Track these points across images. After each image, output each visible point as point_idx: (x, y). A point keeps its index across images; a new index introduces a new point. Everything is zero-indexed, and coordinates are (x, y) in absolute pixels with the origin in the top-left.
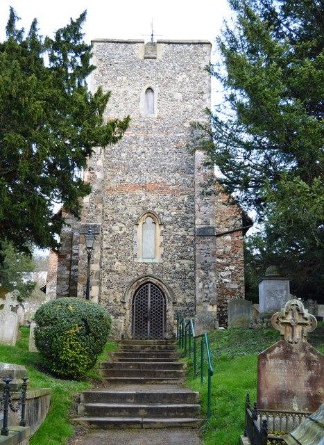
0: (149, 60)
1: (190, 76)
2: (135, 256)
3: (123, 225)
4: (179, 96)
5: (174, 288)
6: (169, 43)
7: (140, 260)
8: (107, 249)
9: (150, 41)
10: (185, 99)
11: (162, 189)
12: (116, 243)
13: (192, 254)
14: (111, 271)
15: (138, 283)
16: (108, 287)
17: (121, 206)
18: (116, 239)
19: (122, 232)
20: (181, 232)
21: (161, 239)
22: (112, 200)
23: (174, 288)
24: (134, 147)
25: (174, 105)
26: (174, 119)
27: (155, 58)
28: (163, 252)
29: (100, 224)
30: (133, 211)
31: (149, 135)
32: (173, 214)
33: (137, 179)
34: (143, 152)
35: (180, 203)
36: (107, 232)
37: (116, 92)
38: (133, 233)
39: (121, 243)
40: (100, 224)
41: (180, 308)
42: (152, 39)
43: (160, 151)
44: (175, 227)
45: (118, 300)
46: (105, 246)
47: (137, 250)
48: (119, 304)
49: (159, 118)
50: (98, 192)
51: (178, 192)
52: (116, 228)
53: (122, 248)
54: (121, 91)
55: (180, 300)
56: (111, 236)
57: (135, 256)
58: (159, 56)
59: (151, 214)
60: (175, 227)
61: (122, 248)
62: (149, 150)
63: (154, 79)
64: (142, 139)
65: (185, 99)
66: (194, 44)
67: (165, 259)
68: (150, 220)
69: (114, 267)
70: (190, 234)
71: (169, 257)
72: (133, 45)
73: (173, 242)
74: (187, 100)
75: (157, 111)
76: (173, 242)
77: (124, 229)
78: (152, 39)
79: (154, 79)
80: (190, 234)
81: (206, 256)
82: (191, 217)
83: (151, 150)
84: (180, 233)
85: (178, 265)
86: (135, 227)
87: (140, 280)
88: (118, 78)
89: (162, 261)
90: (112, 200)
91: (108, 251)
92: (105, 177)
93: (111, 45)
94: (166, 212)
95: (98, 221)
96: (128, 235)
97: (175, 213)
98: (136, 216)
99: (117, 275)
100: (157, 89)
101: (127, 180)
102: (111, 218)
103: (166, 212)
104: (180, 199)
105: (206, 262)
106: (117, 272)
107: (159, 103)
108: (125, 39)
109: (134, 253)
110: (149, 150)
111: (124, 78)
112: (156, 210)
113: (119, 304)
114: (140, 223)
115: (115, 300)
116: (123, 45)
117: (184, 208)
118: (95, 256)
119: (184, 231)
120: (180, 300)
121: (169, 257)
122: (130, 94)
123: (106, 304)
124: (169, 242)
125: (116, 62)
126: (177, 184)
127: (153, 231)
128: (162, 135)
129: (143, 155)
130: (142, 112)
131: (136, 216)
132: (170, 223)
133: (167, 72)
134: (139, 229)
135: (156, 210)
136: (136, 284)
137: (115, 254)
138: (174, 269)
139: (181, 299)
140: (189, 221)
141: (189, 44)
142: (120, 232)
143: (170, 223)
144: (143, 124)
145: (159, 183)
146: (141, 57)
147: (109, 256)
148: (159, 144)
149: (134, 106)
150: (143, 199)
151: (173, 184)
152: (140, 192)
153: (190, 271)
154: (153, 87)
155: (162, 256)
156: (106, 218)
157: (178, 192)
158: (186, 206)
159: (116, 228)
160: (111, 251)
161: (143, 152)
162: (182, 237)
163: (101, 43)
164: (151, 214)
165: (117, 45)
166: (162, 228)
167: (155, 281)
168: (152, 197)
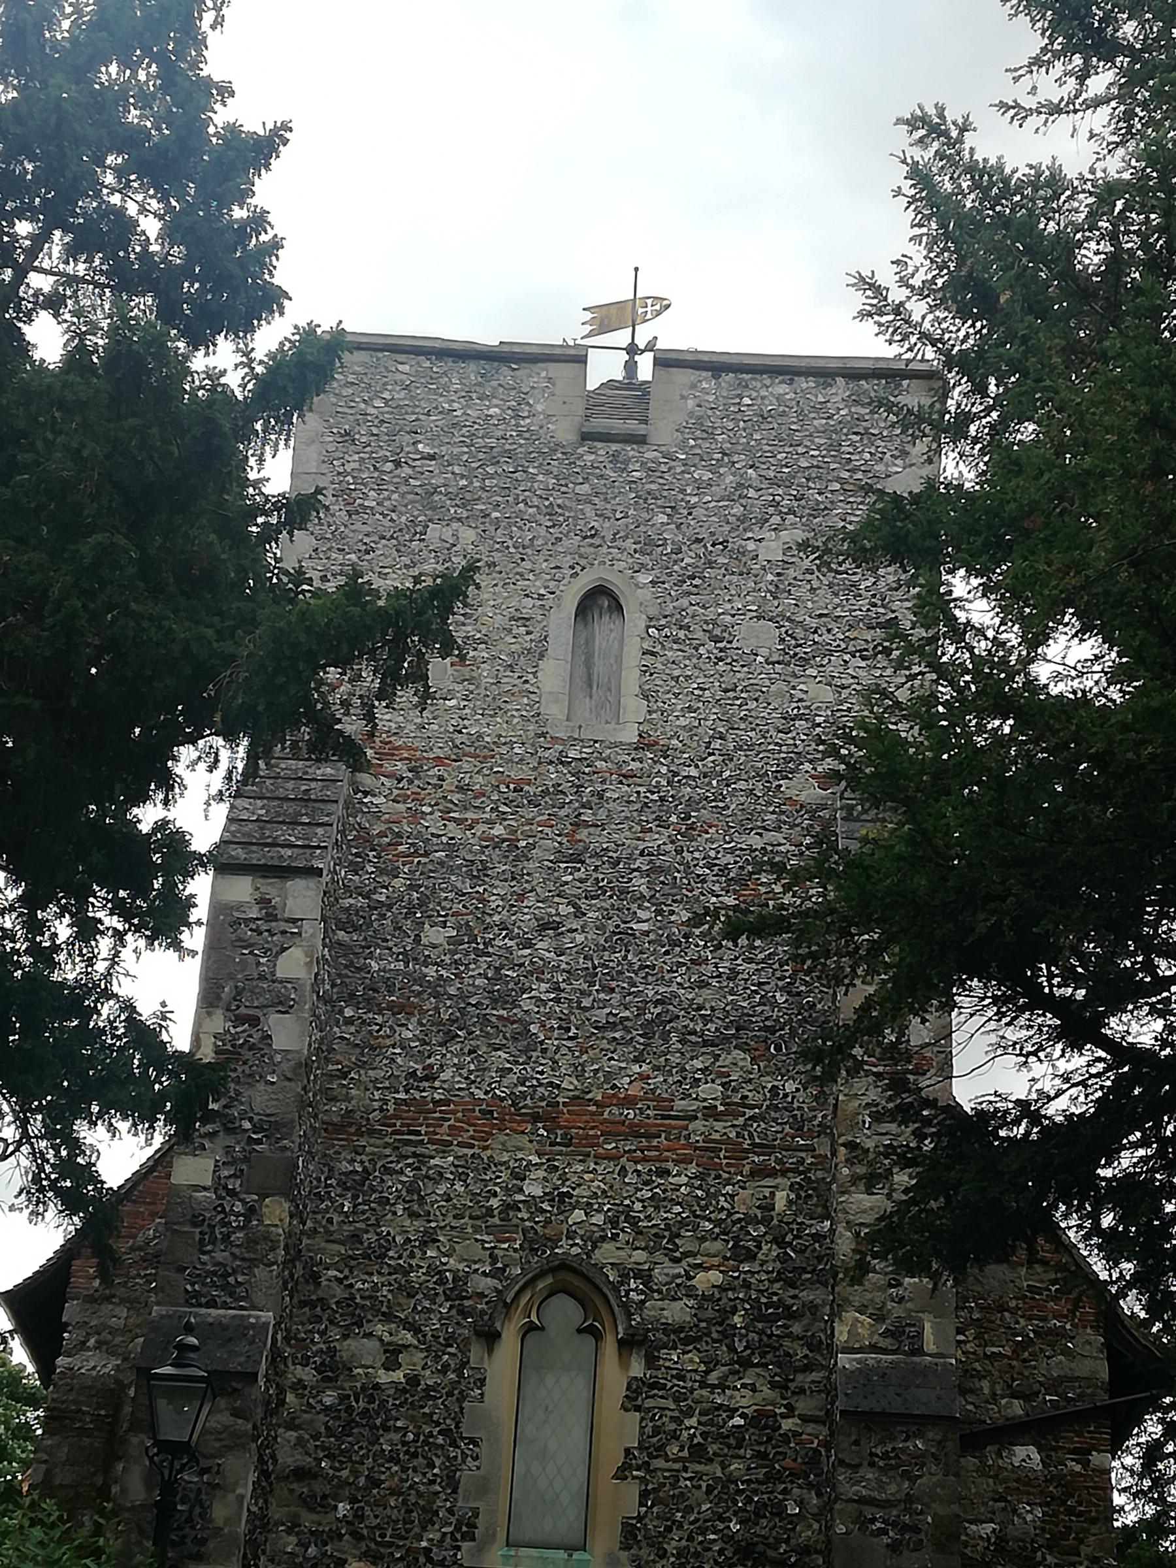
0: (602, 448)
3: (408, 1337)
4: (760, 638)
8: (301, 1474)
9: (619, 375)
10: (795, 657)
11: (647, 1133)
13: (807, 1534)
17: (400, 1225)
18: (362, 1414)
19: (399, 1376)
20: (746, 1397)
21: (623, 1430)
22: (356, 1184)
25: (729, 681)
27: (641, 440)
29: (268, 1316)
30: (467, 1256)
31: (583, 834)
32: (706, 1280)
34: (546, 926)
35: (749, 1219)
38: (466, 1385)
40: (268, 1316)
43: (644, 920)
44: (711, 1363)
46: (288, 1457)
47: (484, 1488)
49: (644, 744)
50: (271, 1128)
51: (738, 1154)
52: (364, 1351)
53: (391, 1475)
58: (664, 429)
59: (574, 1279)
60: (711, 1363)
61: (391, 1475)
62: (579, 913)
63: (629, 544)
64: (545, 851)
65: (795, 657)
67: (646, 1553)
68: (564, 1313)
70: (803, 1405)
71: (672, 1547)
73: (698, 1453)
74: (805, 662)
75: (634, 709)
76: (698, 1453)
79: (629, 544)
80: (803, 1405)
81: (894, 1547)
82: (813, 1308)
86: (476, 1353)
88: (434, 532)
91: (302, 1488)
92: (323, 1050)
94: (664, 1271)
95: (258, 1297)
97: (715, 1277)
98: (486, 1284)
100: (639, 596)
102: (339, 1292)
103: (664, 1271)
104: (746, 1199)
107: (645, 670)
108: (488, 337)
110: (579, 913)
111: (468, 535)
112: (606, 1254)
116: (471, 370)
117: (770, 1251)
118: (220, 1512)
119: (767, 1392)
121: (672, 1547)
124: (673, 1449)
126: (732, 1110)
127: (580, 1384)
128: (657, 840)
130: (554, 711)
131: (486, 1284)
132: (682, 1336)
133: (699, 512)
134: (502, 1365)
135: (606, 1254)
137: (343, 1508)
140: (796, 1328)
142: (383, 1377)
144: (553, 775)
145: (630, 1102)
146: (564, 432)
147: (308, 1520)
149: (510, 680)
151: (710, 1113)
154: (617, 582)
157: (738, 1154)
158: (779, 1241)
160: (319, 1487)
161: (546, 926)
166: (637, 1369)
168: (589, 1178)
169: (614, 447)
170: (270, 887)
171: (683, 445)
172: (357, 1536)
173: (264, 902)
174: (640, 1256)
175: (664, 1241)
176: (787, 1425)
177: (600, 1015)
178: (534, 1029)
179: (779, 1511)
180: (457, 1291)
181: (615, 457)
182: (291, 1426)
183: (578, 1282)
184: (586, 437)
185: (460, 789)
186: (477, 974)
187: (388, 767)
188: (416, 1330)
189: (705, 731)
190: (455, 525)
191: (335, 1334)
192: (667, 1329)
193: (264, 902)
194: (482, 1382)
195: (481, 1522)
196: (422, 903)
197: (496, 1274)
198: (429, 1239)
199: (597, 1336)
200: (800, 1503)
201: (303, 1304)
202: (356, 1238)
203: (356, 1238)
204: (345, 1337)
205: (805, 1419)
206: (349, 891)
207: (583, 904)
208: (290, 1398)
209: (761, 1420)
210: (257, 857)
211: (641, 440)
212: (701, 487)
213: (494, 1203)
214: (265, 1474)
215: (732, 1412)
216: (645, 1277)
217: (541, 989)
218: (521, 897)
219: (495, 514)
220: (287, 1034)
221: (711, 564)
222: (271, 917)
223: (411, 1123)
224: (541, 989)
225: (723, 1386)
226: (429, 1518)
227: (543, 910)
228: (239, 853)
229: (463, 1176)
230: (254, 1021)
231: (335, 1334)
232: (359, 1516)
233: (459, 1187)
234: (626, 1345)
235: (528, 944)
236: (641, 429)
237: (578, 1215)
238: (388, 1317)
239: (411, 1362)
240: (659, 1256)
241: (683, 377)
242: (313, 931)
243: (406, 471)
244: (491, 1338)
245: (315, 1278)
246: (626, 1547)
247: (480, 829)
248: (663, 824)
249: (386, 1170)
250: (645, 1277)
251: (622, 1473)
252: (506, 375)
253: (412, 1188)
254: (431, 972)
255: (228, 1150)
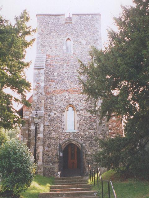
0: (67, 24)
1: (90, 32)
2: (63, 129)
3: (56, 112)
5: (86, 146)
6: (78, 15)
7: (66, 131)
8: (47, 125)
9: (68, 16)
12: (52, 122)
13: (95, 127)
14: (50, 138)
15: (65, 144)
16: (49, 147)
18: (52, 120)
19: (56, 116)
21: (77, 119)
22: (50, 98)
23: (86, 146)
24: (61, 70)
26: (82, 54)
27: (71, 23)
28: (79, 126)
29: (43, 111)
30: (62, 104)
31: (69, 63)
32: (84, 105)
33: (63, 87)
34: (66, 72)
36: (47, 116)
37: (50, 41)
39: (55, 122)
41: (89, 158)
42: (69, 15)
44: (85, 112)
45: (54, 154)
46: (46, 123)
48: (55, 156)
49: (74, 54)
52: (52, 114)
53: (56, 125)
54: (53, 40)
55: (89, 153)
56: (50, 118)
57: (63, 129)
58: (73, 21)
59: (71, 105)
60: (85, 112)
61: (56, 125)
62: (69, 71)
64: (65, 65)
66: (92, 15)
67: (80, 130)
68: (71, 109)
69: (52, 136)
72: (59, 16)
73: (84, 120)
74: (89, 44)
76: (84, 120)
77: (57, 114)
78: (69, 15)
81: (103, 127)
83: (70, 71)
84: (89, 115)
85: (87, 133)
87: (67, 142)
89: (78, 131)
90: (50, 98)
93: (47, 17)
94: (80, 104)
96: (59, 117)
98: (63, 107)
99: (53, 140)
101: (58, 88)
102: (50, 108)
103: (80, 104)
105: (103, 130)
106: (53, 138)
107: (74, 46)
109: (63, 127)
110: (69, 71)
111: (55, 34)
112: (74, 103)
113: (55, 156)
114: (66, 111)
115: (52, 154)
116: (54, 17)
120: (89, 153)
122: (58, 42)
123: (47, 157)
124: (82, 120)
125: (50, 25)
129: (66, 74)
131: (63, 107)
132: (82, 110)
134: (65, 113)
136: (64, 144)
138: (85, 135)
139: (90, 152)
141: (89, 15)
142: (54, 116)
143: (82, 110)
145: (75, 88)
146: (64, 23)
147: (49, 129)
148: (75, 68)
149: (60, 48)
150: (67, 97)
152: (65, 94)
153: (94, 136)
155: (78, 128)
156: (46, 109)
159: (52, 114)
160: (49, 126)
162: (89, 117)
163: (43, 16)
164: (71, 105)
165: (51, 16)
166: (78, 113)
167: (74, 143)
168: (72, 96)
169: (69, 24)
170: (39, 70)
171: (75, 23)
172: (53, 130)
173: (39, 72)
174: (77, 103)
175: (80, 101)
176: (92, 117)
177: (72, 81)
178: (66, 82)
179: (92, 125)
180: (60, 107)
181: (69, 25)
182: (46, 121)
183: (72, 106)
184: (66, 23)
185: (57, 59)
186: (60, 78)
187: (49, 58)
188: (57, 111)
189: (80, 52)
190: (53, 33)
191: (49, 112)
192: (80, 109)
193: (39, 72)
194: (64, 116)
195: (65, 128)
196: (54, 71)
197: (64, 105)
198: (57, 103)
199: (74, 110)
200: (94, 124)
201: (46, 110)
202: (51, 103)
203: (51, 103)
204: (50, 112)
205: (94, 116)
206: (47, 70)
207: (69, 70)
208: (46, 118)
209: (90, 117)
210: (38, 68)
211: (71, 23)
212: (77, 27)
213: (63, 99)
214: (44, 126)
215: (87, 116)
216: (78, 105)
217: (66, 78)
218: (63, 70)
219: (57, 32)
220: (42, 85)
221: (79, 35)
222: (39, 73)
223: (54, 93)
224: (66, 78)
225: (86, 114)
226: (60, 128)
227: (66, 71)
228: (36, 68)
229: (60, 97)
230: (39, 84)
231: (49, 112)
232: (53, 129)
233: (60, 98)
234: (77, 111)
235: (64, 74)
236: (71, 22)
237: (71, 99)
238: (54, 110)
239: (57, 114)
240: (79, 103)
241: (74, 16)
242: (44, 74)
243: (48, 28)
244: (64, 111)
245: (47, 107)
246: (78, 129)
247: (59, 63)
248: (76, 62)
249: (53, 97)
250: (78, 105)
251: (77, 123)
252: (57, 17)
253: (55, 98)
254: (55, 78)
255: (38, 96)
